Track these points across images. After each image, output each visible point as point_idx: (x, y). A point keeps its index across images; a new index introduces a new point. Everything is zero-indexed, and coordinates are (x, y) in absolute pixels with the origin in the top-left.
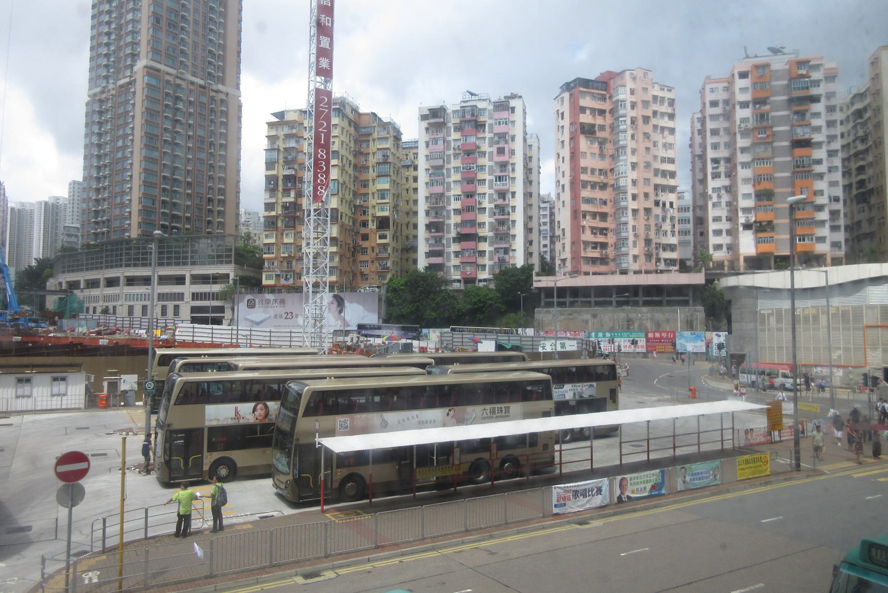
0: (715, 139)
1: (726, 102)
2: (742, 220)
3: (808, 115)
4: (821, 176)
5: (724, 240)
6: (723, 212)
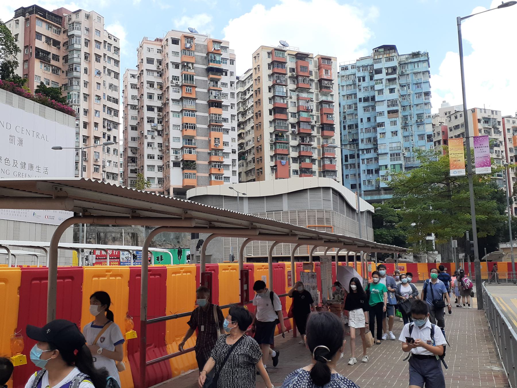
0: (151, 91)
1: (160, 62)
2: (172, 158)
3: (219, 83)
4: (227, 131)
5: (157, 174)
6: (156, 152)
